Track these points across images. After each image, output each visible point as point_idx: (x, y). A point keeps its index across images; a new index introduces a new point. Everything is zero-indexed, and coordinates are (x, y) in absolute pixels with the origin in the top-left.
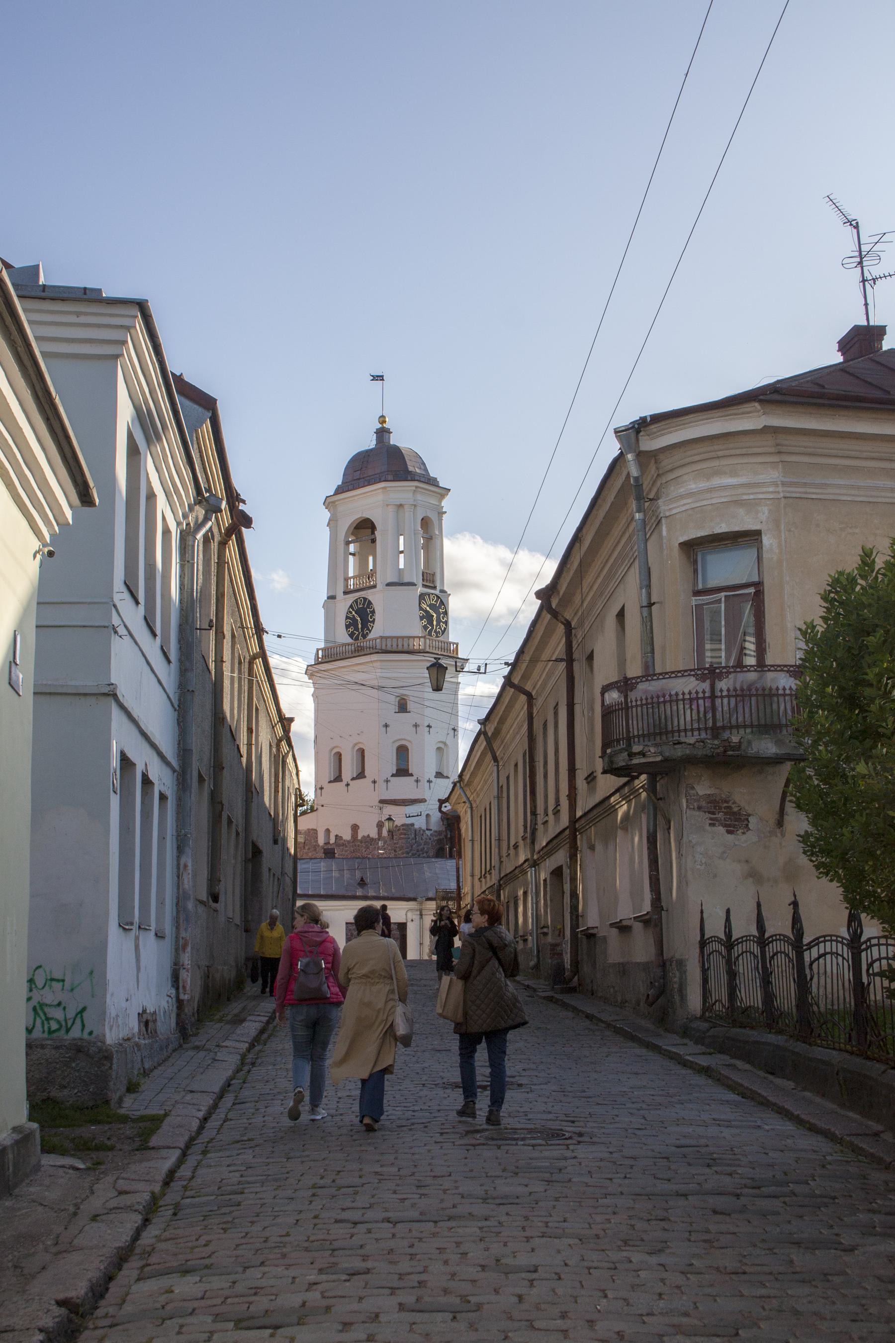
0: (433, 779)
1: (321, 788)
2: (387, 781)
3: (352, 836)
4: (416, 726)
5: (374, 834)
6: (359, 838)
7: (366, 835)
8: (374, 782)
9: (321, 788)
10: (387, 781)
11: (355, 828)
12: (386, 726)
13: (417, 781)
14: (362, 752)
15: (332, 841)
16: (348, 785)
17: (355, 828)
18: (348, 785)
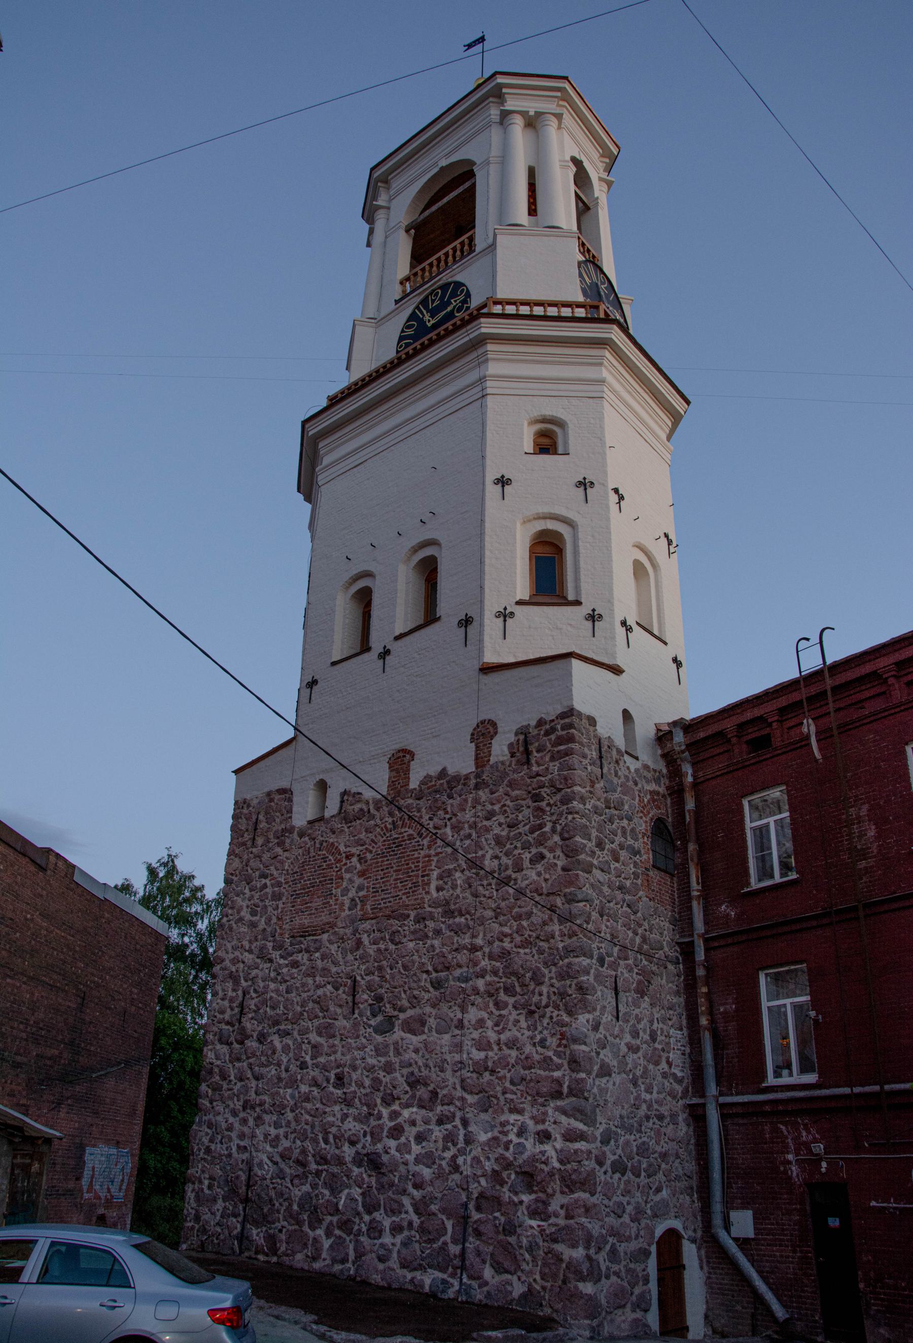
0: (631, 622)
1: (312, 684)
2: (505, 615)
3: (392, 784)
4: (584, 484)
5: (462, 762)
6: (414, 784)
7: (434, 770)
8: (466, 622)
9: (312, 684)
10: (505, 615)
11: (401, 761)
12: (503, 482)
13: (593, 617)
14: (429, 571)
15: (332, 806)
16: (385, 653)
17: (401, 761)
18: (385, 653)
